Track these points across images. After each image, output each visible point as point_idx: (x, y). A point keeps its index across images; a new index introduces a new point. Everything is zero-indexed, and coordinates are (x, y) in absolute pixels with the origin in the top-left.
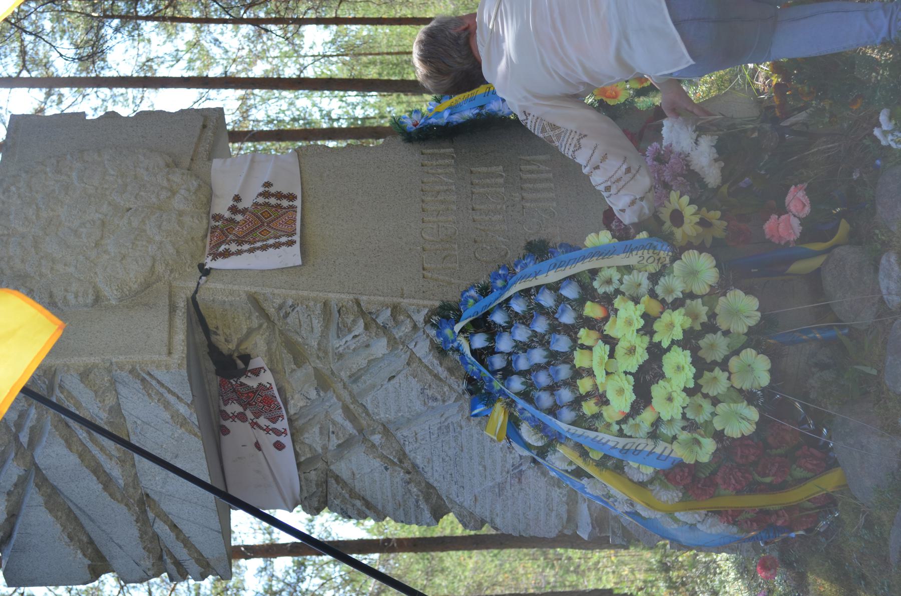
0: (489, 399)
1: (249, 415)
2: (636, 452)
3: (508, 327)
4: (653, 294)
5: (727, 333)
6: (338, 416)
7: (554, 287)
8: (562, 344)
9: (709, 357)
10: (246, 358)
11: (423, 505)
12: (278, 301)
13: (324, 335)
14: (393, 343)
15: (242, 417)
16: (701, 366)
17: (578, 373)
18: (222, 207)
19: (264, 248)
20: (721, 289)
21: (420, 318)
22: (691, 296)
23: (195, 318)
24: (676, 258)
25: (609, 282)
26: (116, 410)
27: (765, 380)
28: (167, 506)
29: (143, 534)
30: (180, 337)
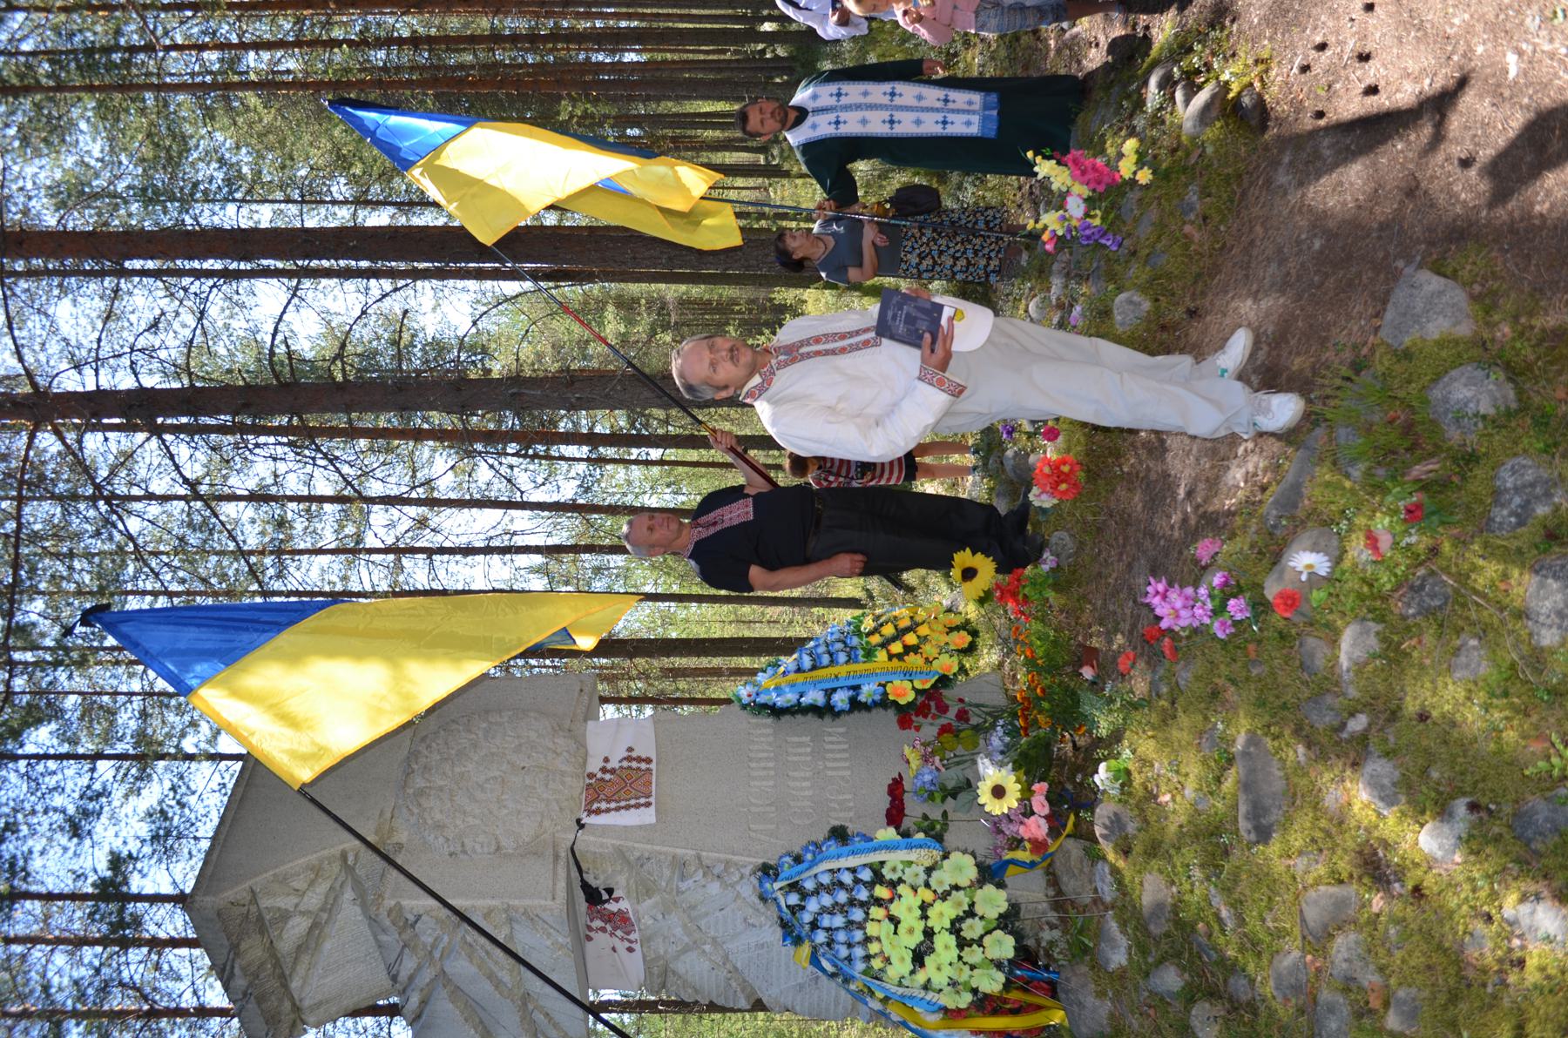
0: (798, 941)
1: (609, 927)
2: (912, 997)
3: (816, 892)
4: (927, 885)
5: (982, 918)
6: (679, 931)
7: (853, 871)
8: (857, 915)
9: (968, 934)
10: (610, 891)
11: (739, 994)
12: (637, 854)
13: (671, 879)
14: (725, 886)
15: (603, 930)
16: (962, 943)
17: (868, 940)
18: (594, 766)
19: (627, 807)
20: (980, 883)
21: (747, 871)
22: (957, 888)
23: (572, 861)
24: (945, 857)
25: (894, 870)
26: (511, 937)
27: (1011, 954)
29: (523, 1019)
30: (562, 884)
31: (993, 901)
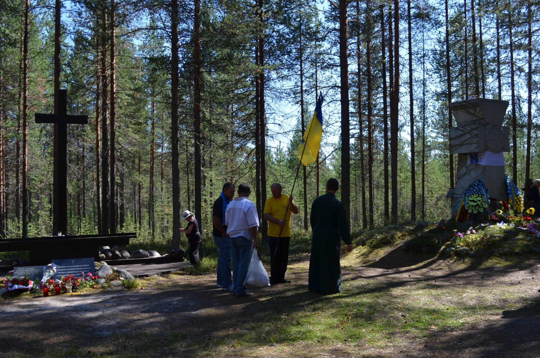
16: (475, 206)
28: (461, 148)
31: (481, 210)
